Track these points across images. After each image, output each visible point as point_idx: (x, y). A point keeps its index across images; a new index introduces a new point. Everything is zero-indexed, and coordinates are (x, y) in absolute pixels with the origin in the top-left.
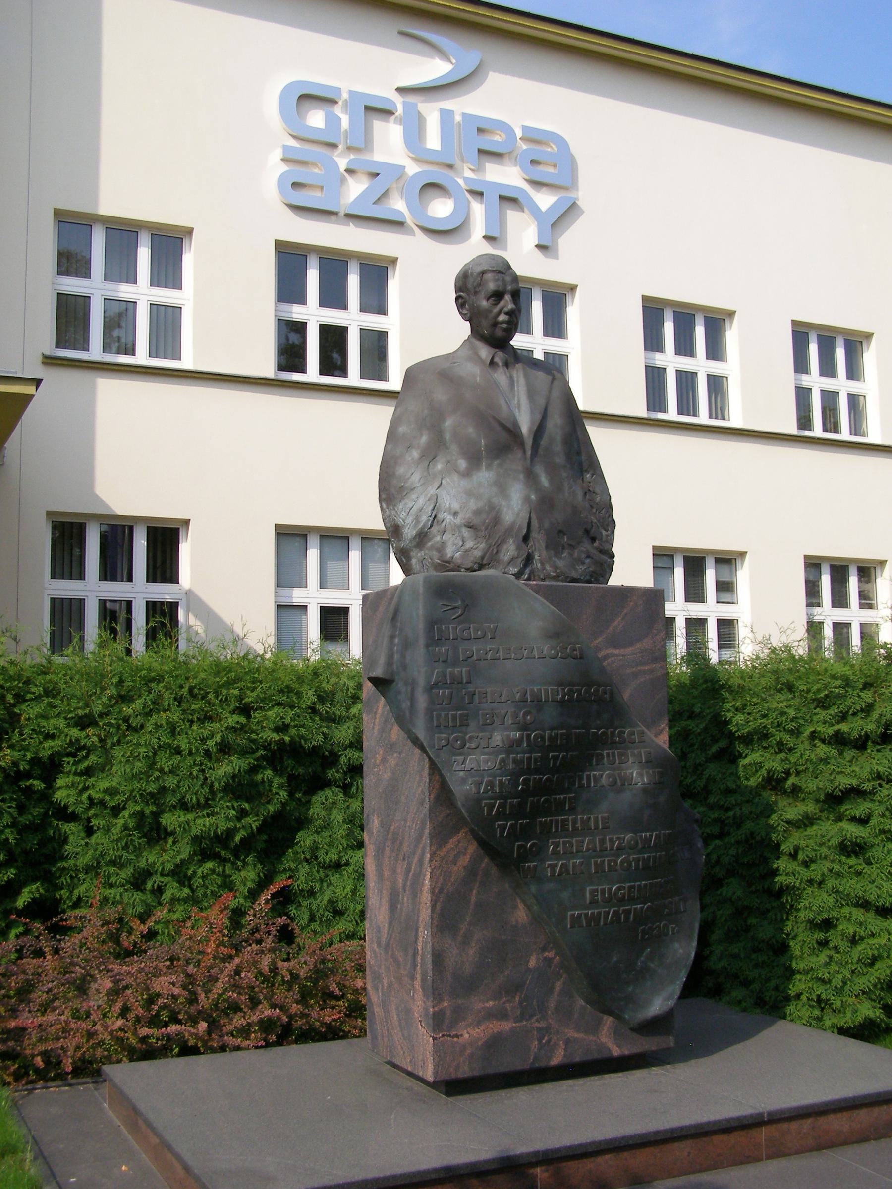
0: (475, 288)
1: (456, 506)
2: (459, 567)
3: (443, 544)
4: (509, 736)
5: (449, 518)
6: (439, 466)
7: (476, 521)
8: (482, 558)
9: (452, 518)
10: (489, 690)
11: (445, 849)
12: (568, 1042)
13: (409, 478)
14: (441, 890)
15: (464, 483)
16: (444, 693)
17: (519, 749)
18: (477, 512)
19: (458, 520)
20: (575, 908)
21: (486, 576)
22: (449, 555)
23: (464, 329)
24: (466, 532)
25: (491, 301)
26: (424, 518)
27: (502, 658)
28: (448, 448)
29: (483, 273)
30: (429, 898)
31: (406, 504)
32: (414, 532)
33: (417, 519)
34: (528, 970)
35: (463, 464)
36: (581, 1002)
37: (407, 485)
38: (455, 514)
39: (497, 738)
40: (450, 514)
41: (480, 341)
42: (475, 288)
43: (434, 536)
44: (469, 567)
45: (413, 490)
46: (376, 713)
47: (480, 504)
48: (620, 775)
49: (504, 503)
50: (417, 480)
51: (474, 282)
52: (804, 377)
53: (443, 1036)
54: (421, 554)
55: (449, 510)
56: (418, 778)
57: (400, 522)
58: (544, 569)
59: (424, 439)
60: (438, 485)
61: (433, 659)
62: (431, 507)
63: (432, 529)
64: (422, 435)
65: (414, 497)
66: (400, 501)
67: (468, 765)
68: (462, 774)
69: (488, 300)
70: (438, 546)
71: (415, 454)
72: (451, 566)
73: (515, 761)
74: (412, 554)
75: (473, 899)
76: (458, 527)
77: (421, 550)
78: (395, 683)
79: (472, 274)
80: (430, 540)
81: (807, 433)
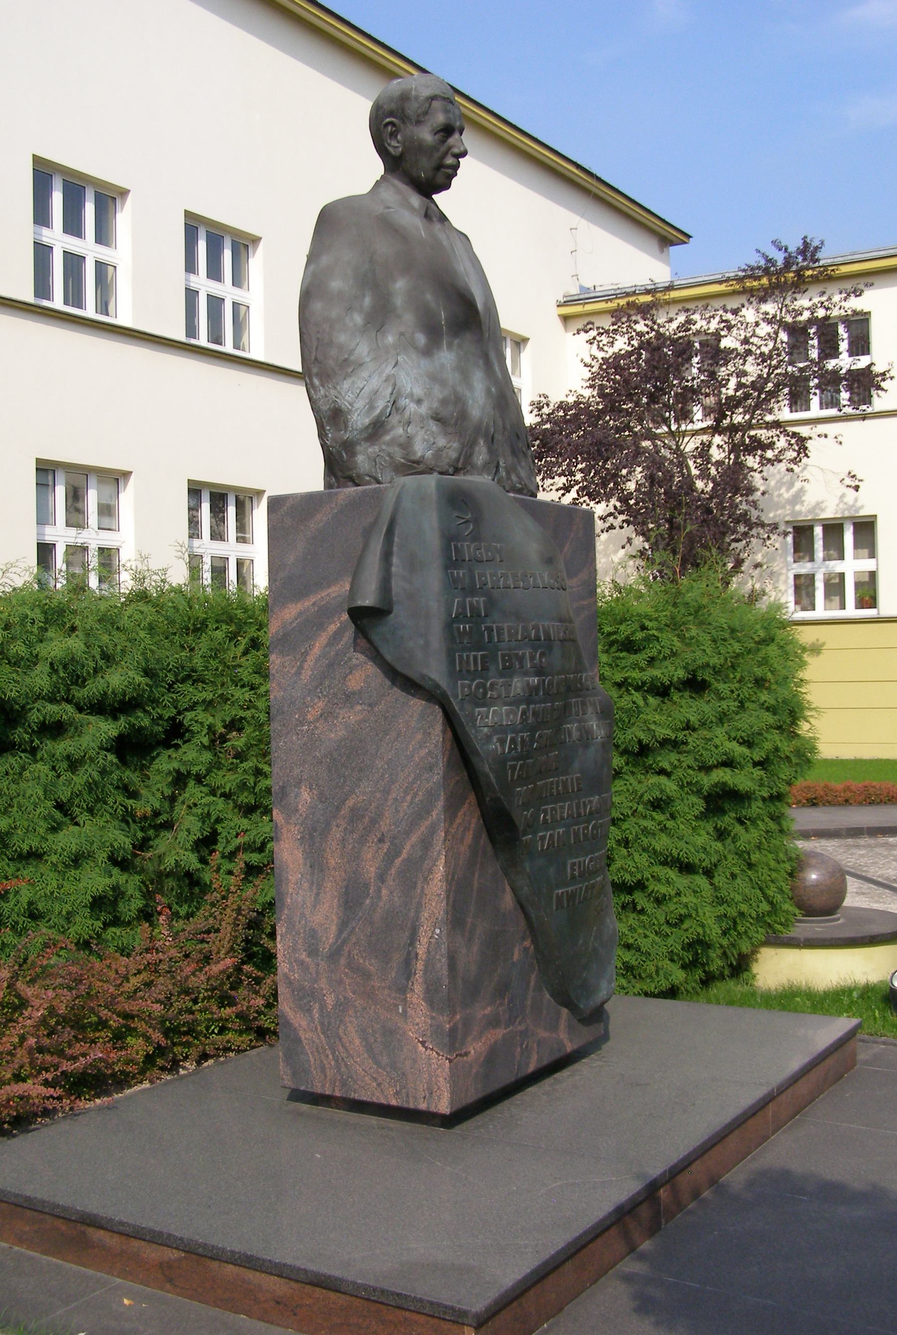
0: (418, 116)
1: (418, 391)
2: (431, 469)
3: (410, 439)
4: (528, 683)
5: (412, 407)
6: (390, 339)
7: (445, 413)
8: (458, 460)
9: (415, 406)
10: (505, 625)
11: (455, 826)
12: (539, 1043)
13: (354, 350)
14: (453, 879)
15: (424, 363)
16: (464, 628)
17: (537, 698)
18: (444, 402)
19: (423, 410)
20: (558, 887)
21: (469, 481)
22: (419, 454)
23: (376, 167)
24: (433, 426)
25: (438, 137)
26: (380, 405)
27: (512, 586)
28: (399, 317)
29: (433, 98)
30: (444, 888)
31: (353, 383)
32: (367, 421)
33: (371, 406)
34: (514, 963)
35: (421, 339)
36: (548, 996)
37: (352, 358)
38: (419, 402)
39: (518, 684)
40: (412, 401)
41: (407, 184)
42: (418, 116)
43: (393, 428)
44: (444, 470)
45: (361, 365)
46: (306, 653)
47: (446, 393)
48: (584, 727)
49: (468, 395)
50: (365, 353)
51: (419, 108)
52: (193, 277)
53: (457, 1056)
54: (373, 450)
55: (411, 396)
56: (419, 736)
57: (344, 404)
58: (509, 478)
59: (367, 301)
60: (393, 364)
61: (452, 584)
62: (390, 390)
63: (390, 418)
64: (364, 296)
65: (365, 374)
66: (345, 379)
67: (490, 721)
68: (486, 730)
69: (435, 134)
70: (402, 440)
71: (358, 319)
72: (421, 467)
73: (535, 714)
74: (359, 448)
75: (476, 885)
76: (422, 419)
77: (373, 444)
78: (392, 616)
79: (417, 98)
80: (387, 432)
81: (193, 341)
